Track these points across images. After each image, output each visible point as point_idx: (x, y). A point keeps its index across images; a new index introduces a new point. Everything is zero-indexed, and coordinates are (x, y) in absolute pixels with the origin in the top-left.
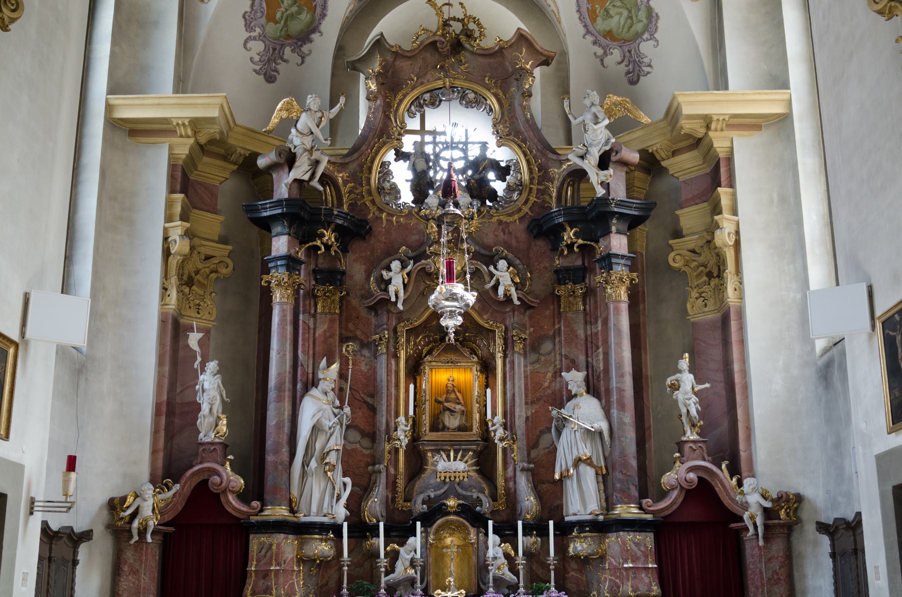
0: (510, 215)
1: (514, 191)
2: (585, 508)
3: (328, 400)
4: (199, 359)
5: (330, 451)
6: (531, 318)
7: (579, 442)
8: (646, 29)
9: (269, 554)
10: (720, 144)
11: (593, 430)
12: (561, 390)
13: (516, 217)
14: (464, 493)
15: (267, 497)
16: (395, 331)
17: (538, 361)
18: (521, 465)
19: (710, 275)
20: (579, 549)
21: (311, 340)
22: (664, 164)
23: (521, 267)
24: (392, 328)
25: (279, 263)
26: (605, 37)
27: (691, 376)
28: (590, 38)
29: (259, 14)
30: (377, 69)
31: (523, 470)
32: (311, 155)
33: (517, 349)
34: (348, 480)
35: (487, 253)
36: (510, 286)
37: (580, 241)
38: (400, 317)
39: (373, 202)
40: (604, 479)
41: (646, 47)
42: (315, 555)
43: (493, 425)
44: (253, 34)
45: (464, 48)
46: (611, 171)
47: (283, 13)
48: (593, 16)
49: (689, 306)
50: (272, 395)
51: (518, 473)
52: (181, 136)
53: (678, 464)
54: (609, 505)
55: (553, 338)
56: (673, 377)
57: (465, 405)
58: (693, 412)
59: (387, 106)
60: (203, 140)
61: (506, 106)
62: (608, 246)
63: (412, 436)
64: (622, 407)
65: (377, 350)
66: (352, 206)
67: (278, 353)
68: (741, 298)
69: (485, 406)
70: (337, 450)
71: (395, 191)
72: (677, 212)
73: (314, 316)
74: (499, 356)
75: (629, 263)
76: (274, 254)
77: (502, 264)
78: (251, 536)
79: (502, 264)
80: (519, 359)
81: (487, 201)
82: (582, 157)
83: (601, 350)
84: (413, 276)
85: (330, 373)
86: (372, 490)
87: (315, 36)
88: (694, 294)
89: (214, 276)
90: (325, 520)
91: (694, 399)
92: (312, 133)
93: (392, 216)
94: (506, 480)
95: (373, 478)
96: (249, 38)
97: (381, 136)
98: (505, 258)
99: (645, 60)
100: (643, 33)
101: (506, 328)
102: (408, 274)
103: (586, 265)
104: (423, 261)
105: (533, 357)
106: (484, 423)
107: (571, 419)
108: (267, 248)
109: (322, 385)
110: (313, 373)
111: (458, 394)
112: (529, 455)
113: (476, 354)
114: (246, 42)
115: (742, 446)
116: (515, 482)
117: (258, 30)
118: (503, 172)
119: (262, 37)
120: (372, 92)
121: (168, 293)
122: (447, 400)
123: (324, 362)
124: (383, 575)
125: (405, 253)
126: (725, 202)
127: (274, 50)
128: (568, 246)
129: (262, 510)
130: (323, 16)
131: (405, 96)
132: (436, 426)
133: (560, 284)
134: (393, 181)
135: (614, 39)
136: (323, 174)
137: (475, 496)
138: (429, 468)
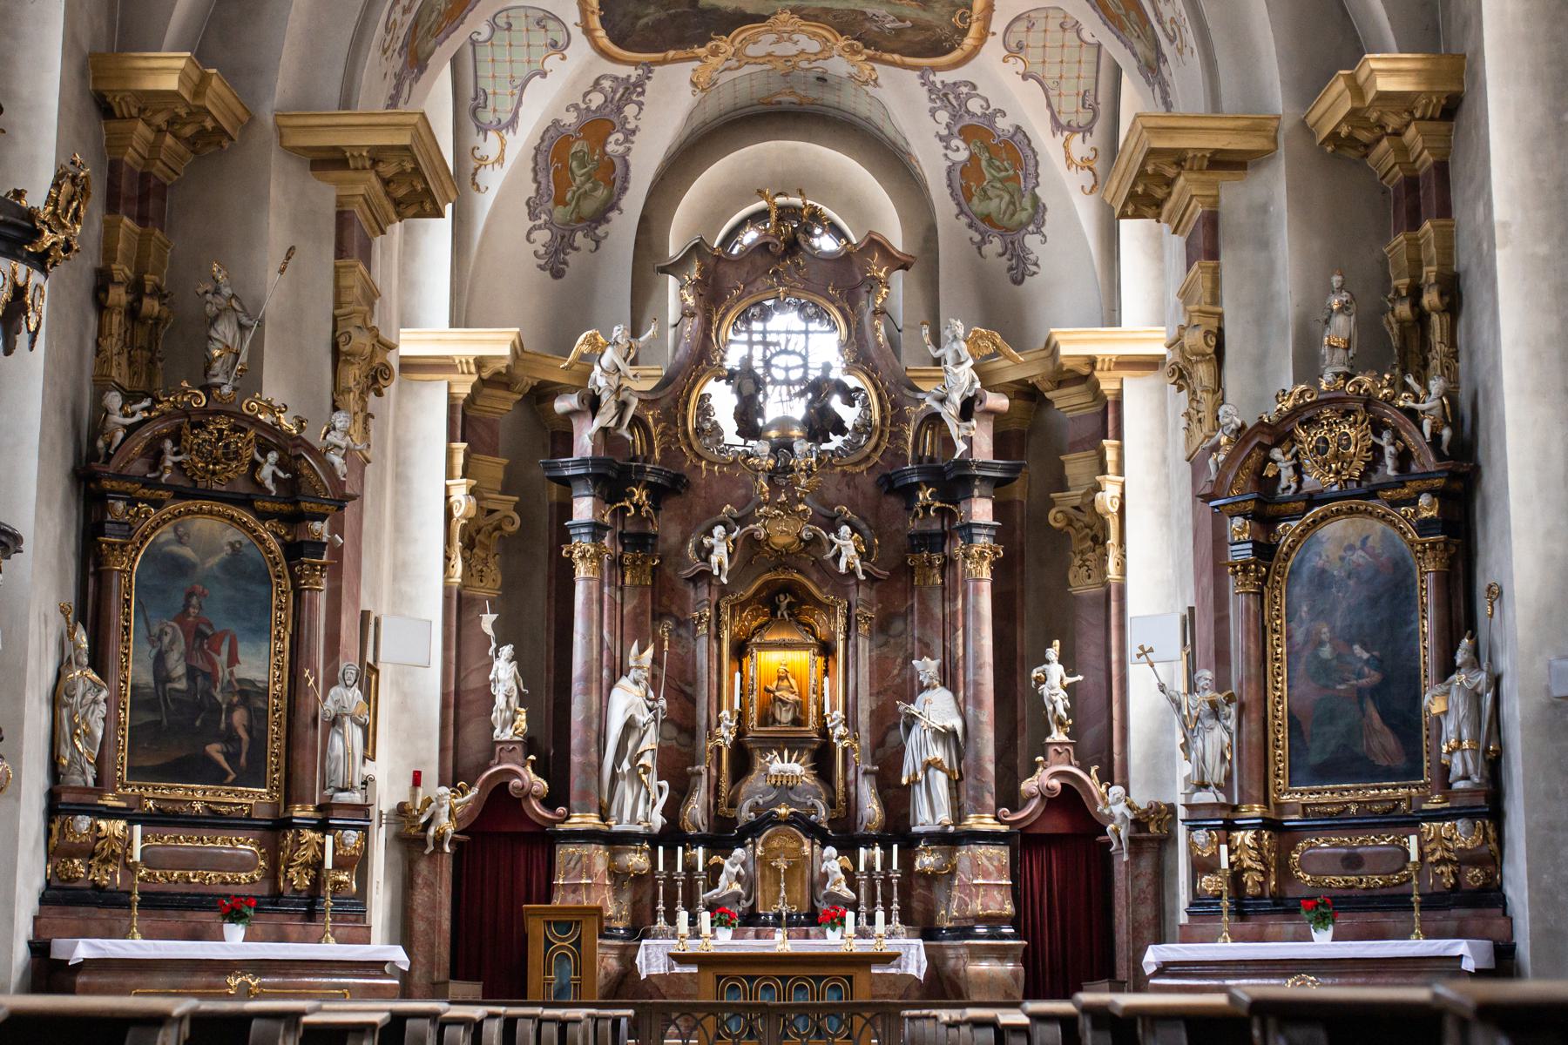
1: (861, 434)
6: (878, 591)
8: (1031, 219)
10: (1107, 386)
13: (863, 467)
14: (797, 799)
15: (574, 802)
16: (717, 607)
17: (886, 644)
18: (863, 767)
19: (1095, 539)
20: (927, 862)
22: (1048, 395)
23: (867, 532)
25: (583, 530)
26: (983, 221)
27: (1060, 668)
28: (964, 220)
29: (545, 198)
30: (695, 275)
31: (866, 773)
32: (618, 396)
34: (665, 783)
35: (827, 512)
36: (853, 557)
37: (938, 504)
38: (724, 591)
39: (690, 446)
40: (955, 785)
41: (1031, 241)
43: (832, 721)
44: (538, 222)
45: (801, 248)
46: (974, 422)
47: (574, 192)
49: (1071, 577)
50: (577, 687)
52: (463, 373)
53: (1040, 769)
54: (958, 814)
55: (904, 616)
56: (1040, 669)
57: (800, 695)
58: (1061, 711)
59: (707, 323)
60: (486, 374)
61: (853, 326)
62: (969, 513)
63: (738, 732)
64: (978, 703)
65: (696, 631)
68: (1123, 572)
71: (717, 430)
72: (1062, 458)
73: (622, 589)
75: (994, 533)
76: (576, 518)
77: (845, 530)
78: (558, 847)
79: (845, 530)
80: (864, 643)
81: (831, 436)
82: (942, 400)
83: (960, 632)
84: (740, 543)
85: (641, 658)
86: (691, 795)
87: (614, 215)
88: (1077, 561)
89: (497, 534)
90: (640, 829)
91: (1063, 694)
93: (714, 464)
94: (846, 785)
95: (693, 780)
96: (534, 228)
97: (699, 363)
98: (848, 523)
99: (1031, 256)
100: (1028, 224)
101: (849, 604)
102: (734, 541)
104: (751, 526)
105: (882, 639)
106: (821, 715)
108: (566, 510)
109: (633, 674)
111: (792, 681)
112: (873, 755)
113: (814, 634)
114: (529, 233)
115: (1116, 749)
117: (544, 217)
120: (688, 307)
121: (452, 563)
122: (778, 689)
123: (635, 648)
125: (730, 512)
126: (1111, 456)
127: (563, 237)
128: (922, 507)
129: (568, 818)
130: (624, 189)
131: (728, 310)
132: (766, 718)
133: (914, 552)
134: (713, 419)
135: (993, 224)
136: (634, 417)
137: (809, 803)
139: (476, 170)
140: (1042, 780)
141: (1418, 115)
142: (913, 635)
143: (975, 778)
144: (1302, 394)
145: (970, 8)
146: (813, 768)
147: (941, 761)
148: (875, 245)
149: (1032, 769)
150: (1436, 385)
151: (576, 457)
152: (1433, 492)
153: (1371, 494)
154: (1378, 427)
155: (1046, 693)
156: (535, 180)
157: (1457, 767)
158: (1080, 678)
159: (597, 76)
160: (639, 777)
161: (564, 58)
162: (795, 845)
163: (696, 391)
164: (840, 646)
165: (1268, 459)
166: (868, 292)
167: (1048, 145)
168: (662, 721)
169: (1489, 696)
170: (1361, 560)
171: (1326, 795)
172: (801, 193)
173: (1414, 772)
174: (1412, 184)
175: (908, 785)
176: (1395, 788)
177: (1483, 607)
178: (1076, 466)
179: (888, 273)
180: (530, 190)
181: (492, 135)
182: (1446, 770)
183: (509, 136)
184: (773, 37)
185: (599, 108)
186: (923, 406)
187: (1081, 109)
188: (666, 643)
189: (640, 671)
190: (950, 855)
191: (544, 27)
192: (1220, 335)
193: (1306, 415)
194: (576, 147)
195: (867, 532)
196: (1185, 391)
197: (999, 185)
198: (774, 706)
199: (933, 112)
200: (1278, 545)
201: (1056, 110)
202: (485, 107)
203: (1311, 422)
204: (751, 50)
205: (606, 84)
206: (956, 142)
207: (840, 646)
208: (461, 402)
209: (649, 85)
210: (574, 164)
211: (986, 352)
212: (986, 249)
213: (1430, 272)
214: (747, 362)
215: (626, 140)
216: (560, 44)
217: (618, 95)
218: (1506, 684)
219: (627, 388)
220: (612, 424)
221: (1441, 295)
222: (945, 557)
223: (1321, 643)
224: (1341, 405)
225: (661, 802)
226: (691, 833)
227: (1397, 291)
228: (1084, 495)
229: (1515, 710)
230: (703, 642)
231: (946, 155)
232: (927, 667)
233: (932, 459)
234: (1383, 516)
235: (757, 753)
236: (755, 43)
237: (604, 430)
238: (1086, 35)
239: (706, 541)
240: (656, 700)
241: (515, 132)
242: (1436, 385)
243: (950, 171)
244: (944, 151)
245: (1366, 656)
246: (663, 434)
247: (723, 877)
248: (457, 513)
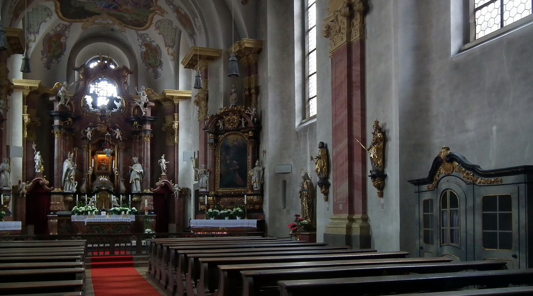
0: (120, 115)
2: (137, 190)
4: (35, 151)
10: (176, 102)
12: (132, 161)
13: (121, 116)
16: (88, 145)
19: (172, 134)
21: (65, 146)
22: (162, 103)
23: (122, 130)
24: (87, 144)
25: (56, 127)
28: (144, 64)
30: (83, 71)
31: (122, 181)
33: (121, 151)
34: (76, 182)
37: (139, 125)
39: (82, 110)
40: (141, 183)
41: (159, 70)
43: (114, 170)
44: (44, 56)
46: (147, 108)
48: (145, 58)
49: (166, 141)
50: (55, 161)
51: (120, 182)
54: (142, 189)
56: (160, 160)
57: (107, 164)
60: (32, 90)
62: (145, 127)
64: (147, 167)
66: (76, 110)
67: (57, 150)
71: (88, 106)
72: (165, 116)
76: (55, 124)
77: (118, 130)
79: (118, 130)
82: (140, 103)
86: (82, 185)
87: (62, 56)
88: (168, 138)
92: (65, 92)
94: (117, 183)
103: (140, 130)
109: (69, 159)
110: (66, 155)
114: (42, 59)
116: (120, 183)
118: (118, 101)
119: (46, 57)
122: (102, 162)
125: (91, 124)
126: (176, 117)
128: (135, 125)
130: (65, 50)
134: (87, 104)
136: (68, 102)
139: (28, 43)
140: (161, 182)
141: (252, 52)
144: (225, 109)
145: (148, 17)
146: (110, 179)
147: (139, 178)
148: (125, 68)
149: (158, 181)
150: (254, 109)
151: (55, 110)
152: (252, 131)
153: (239, 131)
154: (241, 117)
155: (161, 165)
156: (43, 46)
157: (255, 185)
158: (168, 162)
159: (59, 23)
160: (71, 181)
161: (51, 18)
162: (106, 195)
163: (83, 97)
164: (116, 154)
165: (217, 122)
166: (123, 78)
167: (164, 50)
168: (76, 169)
169: (262, 172)
170: (236, 144)
171: (227, 190)
172: (108, 55)
173: (245, 186)
174: (249, 66)
176: (241, 189)
177: (261, 154)
178: (168, 119)
179: (127, 74)
180: (42, 49)
181: (32, 35)
182: (253, 186)
183: (37, 36)
184: (102, 19)
185: (59, 31)
186: (135, 104)
187: (171, 42)
188: (76, 153)
189: (70, 158)
190: (140, 198)
191: (46, 10)
192: (207, 95)
193: (226, 113)
194: (53, 39)
195: (122, 130)
196: (198, 106)
197: (152, 57)
198: (101, 166)
199: (138, 40)
200: (219, 139)
201: (166, 42)
202: (31, 27)
203: (227, 115)
204: (96, 21)
205: (61, 26)
206: (143, 47)
207: (116, 154)
208: (26, 96)
209: (71, 27)
210: (53, 44)
211: (150, 93)
212: (149, 71)
213: (253, 85)
214: (94, 92)
215: (65, 39)
216: (50, 15)
217: (64, 29)
218: (266, 170)
219: (67, 96)
220: (63, 104)
221: (255, 90)
222: (140, 136)
223: (227, 160)
224: (234, 112)
227: (245, 89)
228: (170, 124)
229: (267, 175)
230: (85, 152)
231: (141, 50)
232: (135, 159)
233: (137, 115)
234: (241, 135)
235: (97, 176)
236: (97, 20)
237: (61, 105)
238: (173, 26)
239: (86, 131)
240: (74, 164)
241: (38, 35)
242: (254, 109)
243: (141, 53)
244: (140, 48)
245: (236, 163)
246: (75, 106)
248: (26, 121)
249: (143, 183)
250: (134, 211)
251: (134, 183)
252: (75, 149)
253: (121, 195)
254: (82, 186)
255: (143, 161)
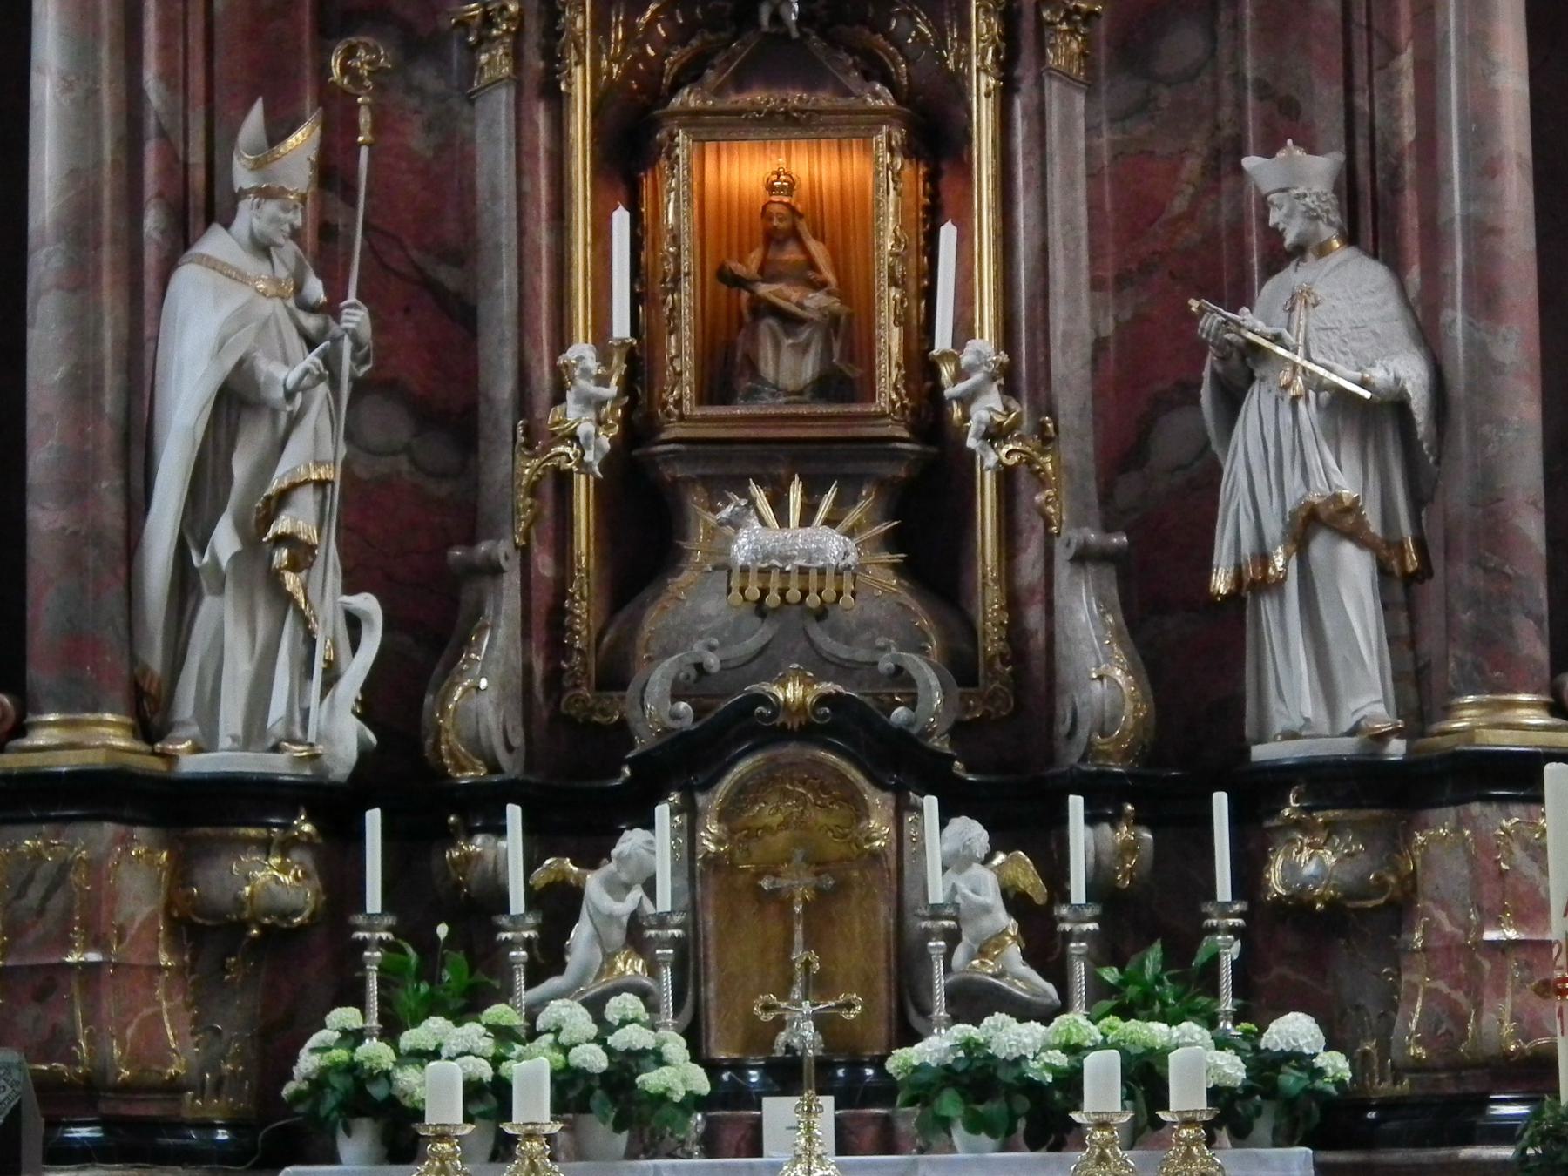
3: (276, 281)
5: (294, 487)
7: (1310, 445)
9: (57, 902)
11: (1367, 395)
12: (1238, 232)
14: (843, 652)
15: (39, 675)
17: (1143, 107)
20: (1310, 869)
31: (1082, 557)
34: (367, 604)
42: (239, 903)
43: (960, 375)
51: (1063, 572)
57: (844, 292)
63: (626, 422)
65: (472, 68)
67: (67, 85)
69: (930, 294)
70: (321, 484)
74: (983, 85)
80: (1067, 103)
83: (1406, 60)
86: (465, 643)
90: (279, 765)
94: (1013, 602)
95: (467, 596)
107: (1280, 350)
109: (248, 217)
112: (1106, 497)
113: (887, 80)
122: (768, 272)
123: (255, 120)
124: (520, 978)
129: (20, 730)
137: (885, 664)
138: (697, 543)
142: (1238, 78)
143: (1477, 562)
147: (1353, 508)
162: (833, 817)
168: (359, 386)
175: (1235, 598)
188: (364, 118)
189: (271, 207)
190: (1395, 840)
198: (754, 338)
225: (357, 669)
226: (466, 777)
230: (499, 106)
235: (695, 500)
240: (331, 309)
247: (581, 935)
249: (1434, 587)
250: (1290, 1079)
251: (1280, 583)
252: (350, 53)
253: (1076, 804)
254: (450, 671)
255: (1411, 221)
